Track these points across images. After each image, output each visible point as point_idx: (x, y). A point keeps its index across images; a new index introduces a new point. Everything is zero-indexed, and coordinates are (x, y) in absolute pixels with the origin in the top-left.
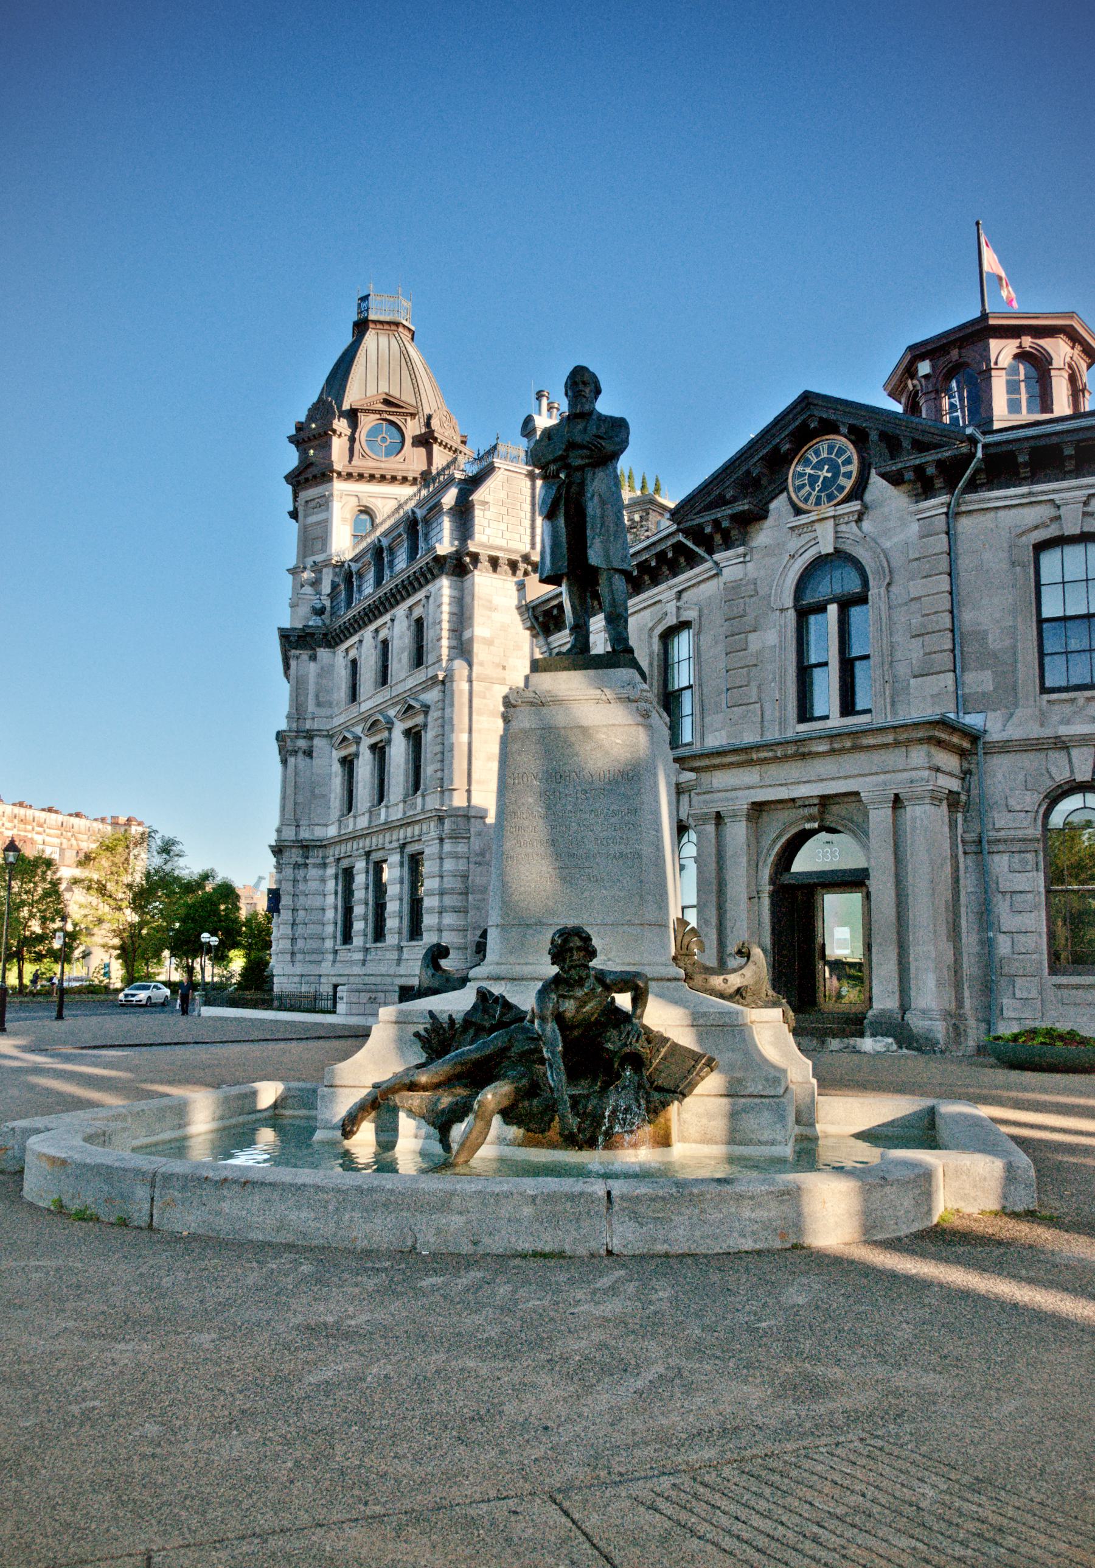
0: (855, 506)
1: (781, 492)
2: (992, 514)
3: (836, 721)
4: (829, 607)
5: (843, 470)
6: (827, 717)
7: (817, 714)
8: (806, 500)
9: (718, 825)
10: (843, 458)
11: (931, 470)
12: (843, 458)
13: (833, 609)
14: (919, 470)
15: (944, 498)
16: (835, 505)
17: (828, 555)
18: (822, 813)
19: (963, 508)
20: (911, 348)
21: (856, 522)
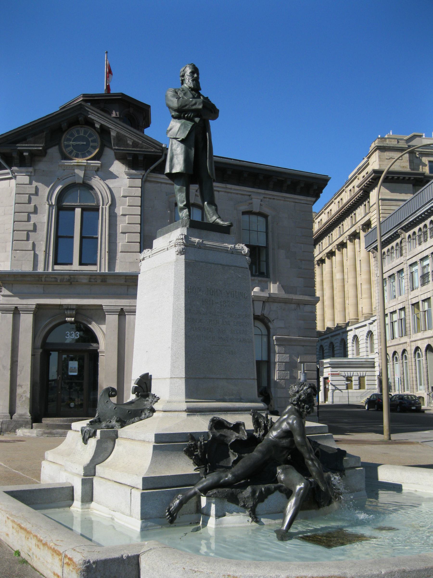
0: (97, 163)
1: (55, 146)
2: (159, 184)
3: (76, 266)
4: (76, 209)
5: (91, 144)
6: (71, 264)
7: (59, 262)
8: (71, 153)
9: (14, 314)
10: (92, 138)
11: (141, 158)
12: (92, 138)
13: (78, 211)
14: (135, 156)
15: (143, 172)
16: (87, 160)
17: (78, 184)
18: (76, 313)
19: (149, 179)
20: (84, 95)
21: (96, 171)
